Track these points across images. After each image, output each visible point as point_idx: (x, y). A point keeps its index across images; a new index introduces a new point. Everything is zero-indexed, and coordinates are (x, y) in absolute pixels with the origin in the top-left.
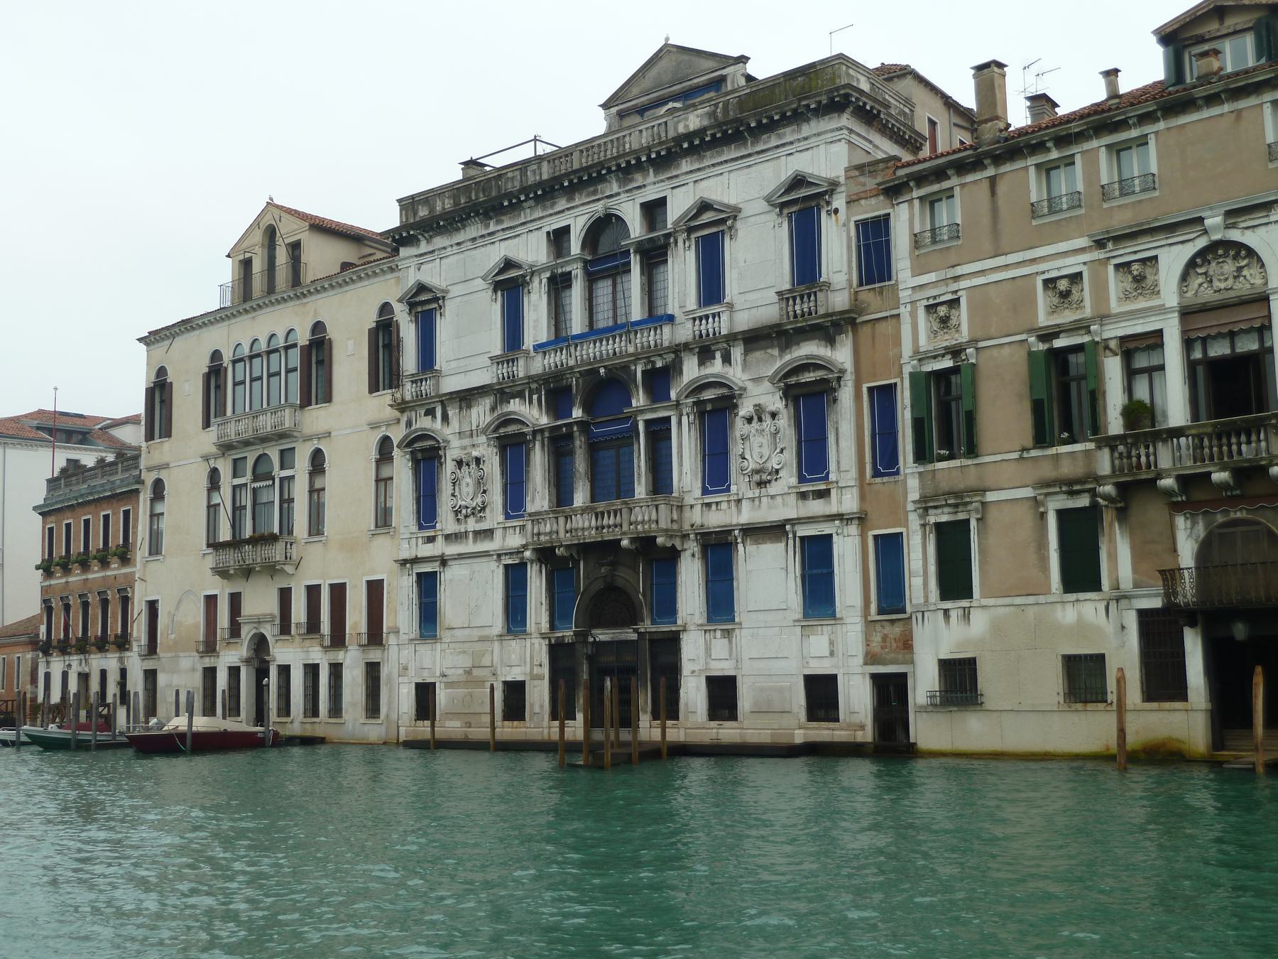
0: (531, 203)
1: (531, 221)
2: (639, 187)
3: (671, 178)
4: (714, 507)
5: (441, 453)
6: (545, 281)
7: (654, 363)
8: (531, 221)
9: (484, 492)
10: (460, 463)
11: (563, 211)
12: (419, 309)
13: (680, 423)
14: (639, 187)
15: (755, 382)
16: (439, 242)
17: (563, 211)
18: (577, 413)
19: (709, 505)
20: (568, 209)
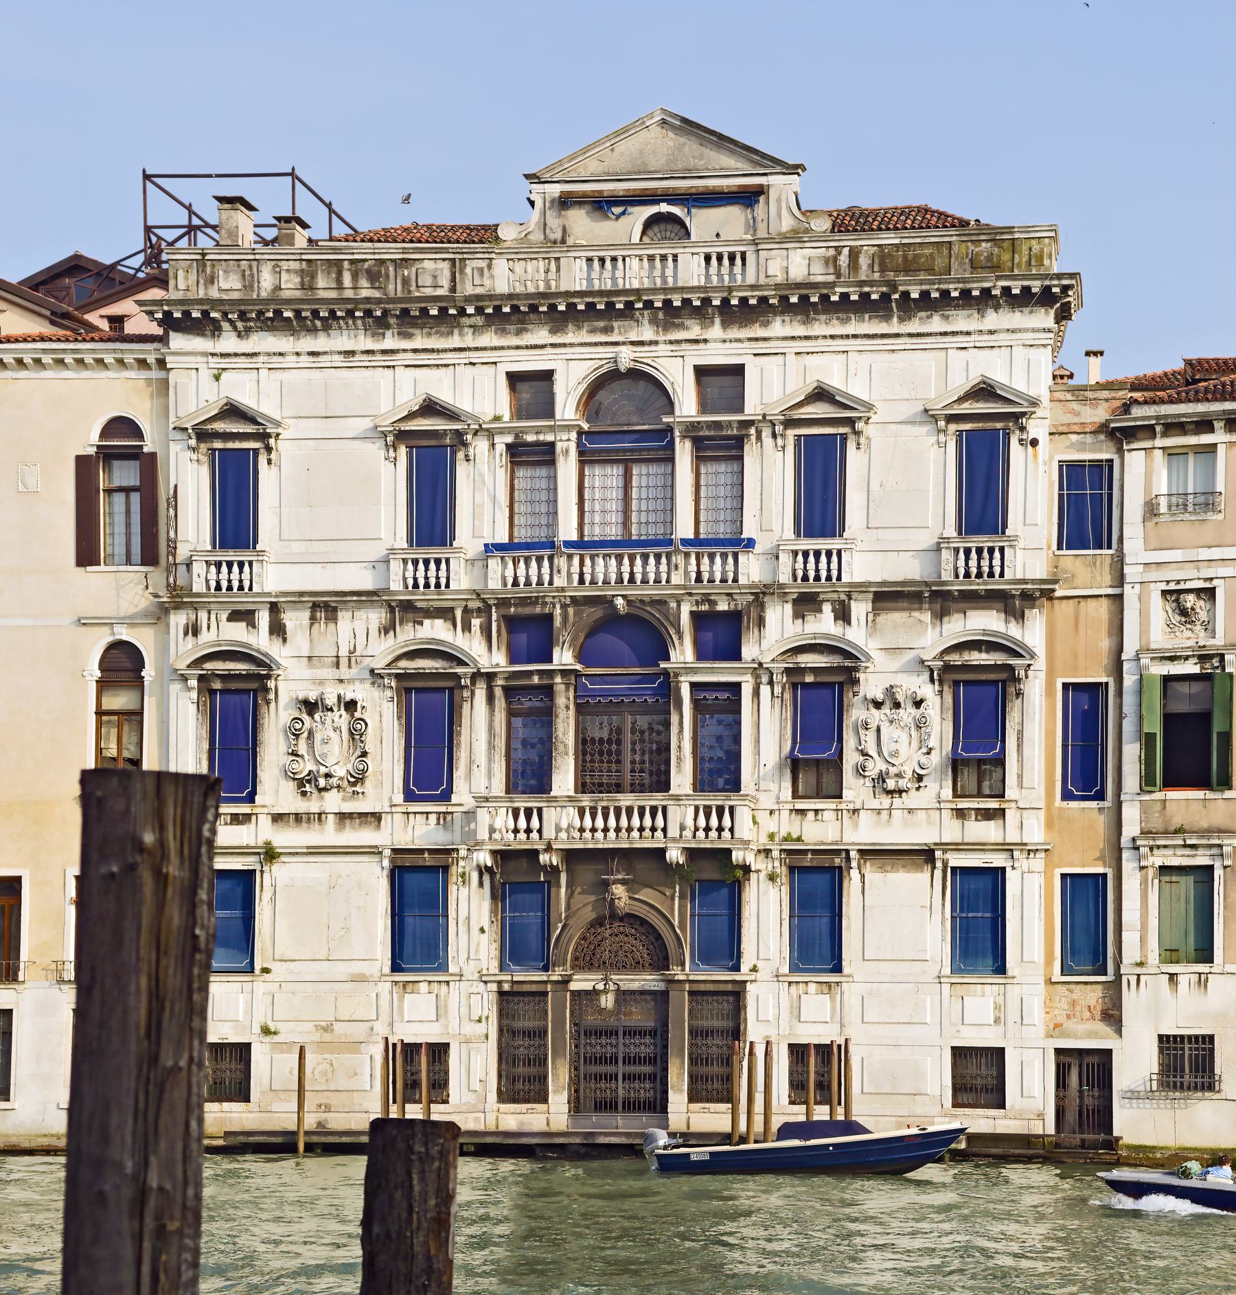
0: (479, 321)
1: (477, 349)
2: (696, 341)
3: (756, 339)
4: (811, 815)
5: (271, 684)
6: (501, 448)
7: (713, 603)
8: (477, 349)
9: (364, 754)
10: (310, 707)
11: (543, 347)
12: (218, 445)
13: (756, 693)
14: (696, 341)
15: (896, 656)
16: (263, 342)
17: (543, 347)
18: (564, 657)
19: (802, 812)
20: (553, 345)
